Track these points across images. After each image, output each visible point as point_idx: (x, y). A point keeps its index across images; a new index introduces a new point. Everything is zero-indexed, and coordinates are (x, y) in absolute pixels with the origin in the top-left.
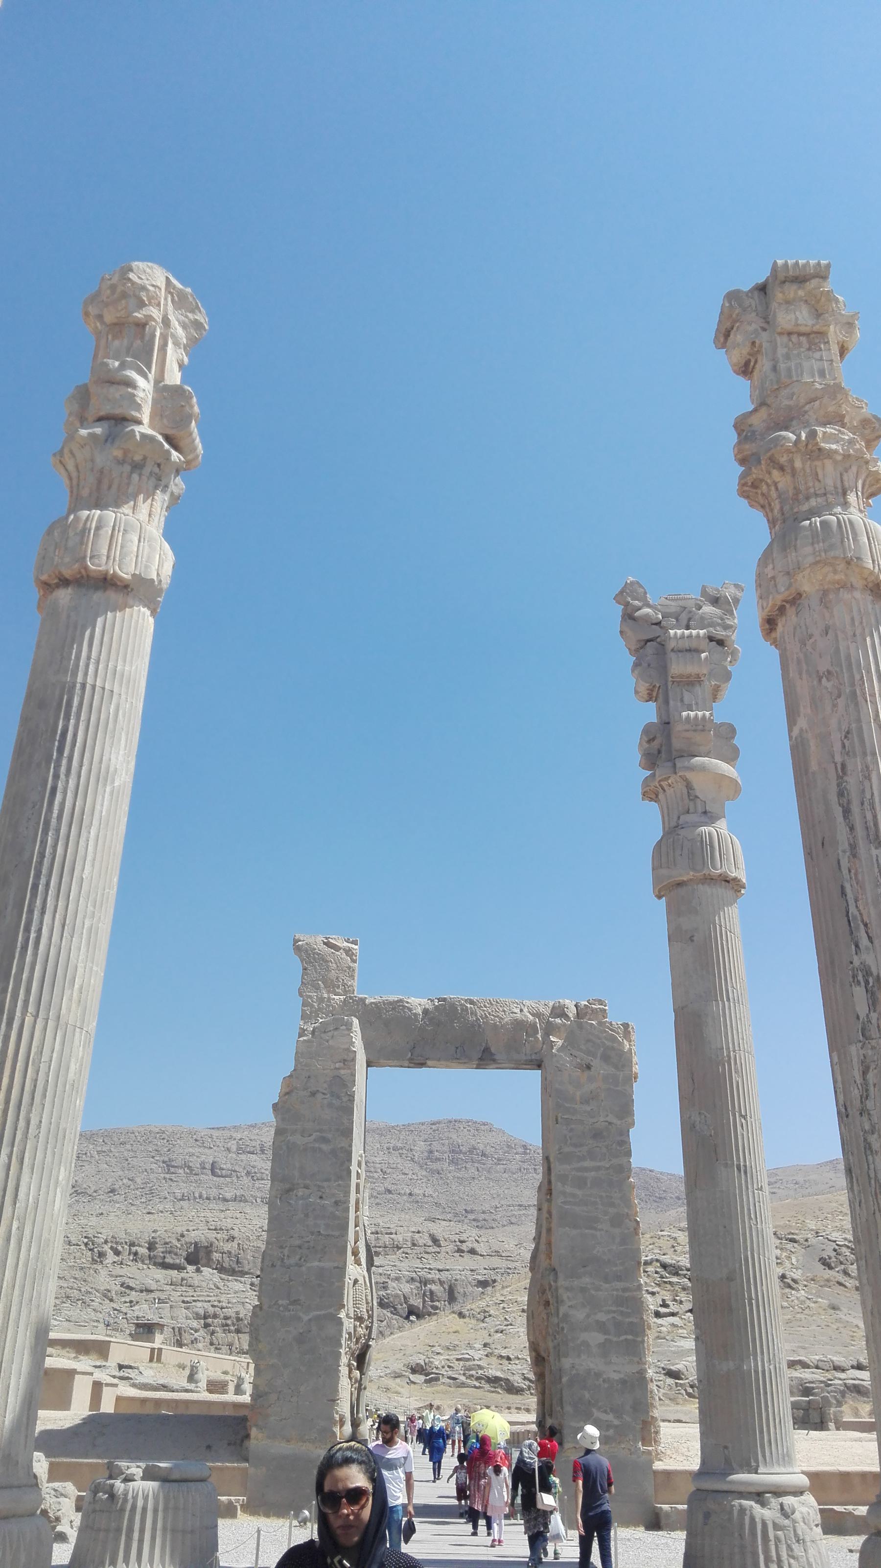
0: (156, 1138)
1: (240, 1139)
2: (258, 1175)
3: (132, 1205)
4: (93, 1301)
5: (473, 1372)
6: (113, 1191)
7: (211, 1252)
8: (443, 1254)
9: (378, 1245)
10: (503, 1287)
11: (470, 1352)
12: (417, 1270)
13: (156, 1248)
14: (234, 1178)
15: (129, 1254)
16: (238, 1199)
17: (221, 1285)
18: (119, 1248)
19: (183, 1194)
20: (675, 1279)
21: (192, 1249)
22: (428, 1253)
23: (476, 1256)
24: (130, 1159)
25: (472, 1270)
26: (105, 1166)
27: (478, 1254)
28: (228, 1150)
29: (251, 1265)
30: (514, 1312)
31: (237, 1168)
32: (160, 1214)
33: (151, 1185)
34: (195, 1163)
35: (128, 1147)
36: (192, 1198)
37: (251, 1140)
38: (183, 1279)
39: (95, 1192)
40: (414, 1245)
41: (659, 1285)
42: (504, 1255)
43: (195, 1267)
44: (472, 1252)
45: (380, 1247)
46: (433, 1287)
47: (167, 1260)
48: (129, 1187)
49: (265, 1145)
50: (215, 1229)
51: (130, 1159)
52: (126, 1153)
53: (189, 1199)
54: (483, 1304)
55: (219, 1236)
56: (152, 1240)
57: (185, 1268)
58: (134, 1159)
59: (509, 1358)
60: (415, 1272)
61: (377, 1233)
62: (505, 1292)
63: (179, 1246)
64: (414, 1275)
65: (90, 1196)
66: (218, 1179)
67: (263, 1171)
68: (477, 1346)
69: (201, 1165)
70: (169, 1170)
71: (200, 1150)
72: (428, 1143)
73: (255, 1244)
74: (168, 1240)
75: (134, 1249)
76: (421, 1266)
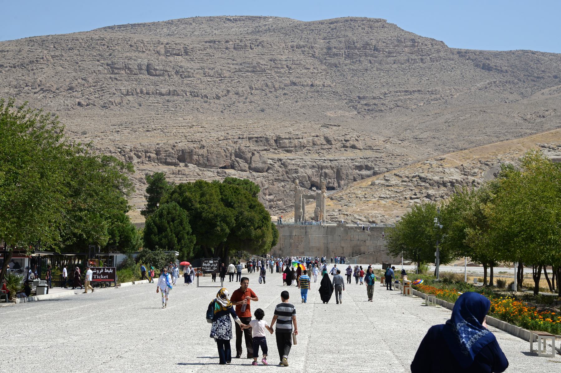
0: (97, 44)
1: (167, 44)
2: (185, 74)
3: (89, 99)
4: (136, 184)
5: (334, 220)
6: (71, 89)
7: (192, 155)
8: (333, 150)
9: (291, 146)
10: (351, 187)
11: (333, 213)
12: (316, 161)
13: (161, 154)
14: (167, 77)
15: (146, 157)
16: (172, 93)
17: (200, 173)
18: (140, 154)
19: (128, 90)
20: (423, 184)
21: (181, 153)
22: (324, 149)
23: (355, 150)
24: (80, 63)
25: (352, 160)
26: (61, 68)
27: (357, 149)
28: (158, 52)
29: (216, 162)
30: (353, 198)
31: (168, 69)
32: (155, 131)
33: (101, 84)
34: (133, 65)
35: (76, 52)
36: (135, 93)
37: (176, 44)
38: (179, 171)
39: (57, 89)
40: (314, 144)
41: (415, 187)
42: (374, 148)
43: (184, 164)
44: (353, 147)
45: (292, 147)
46: (327, 171)
47: (168, 160)
48: (84, 85)
49: (188, 48)
50: (192, 141)
51: (80, 63)
52: (75, 58)
53: (132, 94)
54: (340, 194)
55: (195, 145)
56: (158, 149)
57: (179, 165)
58: (83, 62)
59: (347, 215)
60: (315, 162)
61: (290, 139)
62: (351, 189)
63: (174, 152)
64: (314, 164)
65: (54, 92)
66: (153, 78)
67: (189, 70)
68: (336, 211)
69: (138, 66)
70: (113, 71)
71: (135, 54)
72: (327, 41)
73: (216, 150)
74: (167, 149)
75: (148, 154)
76: (319, 158)
